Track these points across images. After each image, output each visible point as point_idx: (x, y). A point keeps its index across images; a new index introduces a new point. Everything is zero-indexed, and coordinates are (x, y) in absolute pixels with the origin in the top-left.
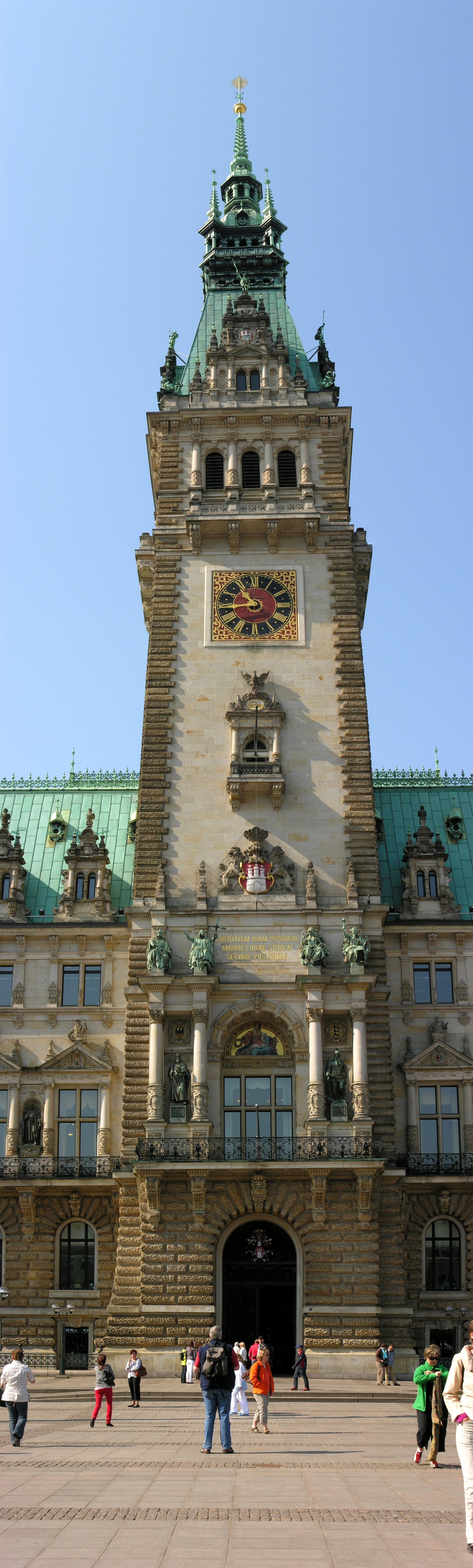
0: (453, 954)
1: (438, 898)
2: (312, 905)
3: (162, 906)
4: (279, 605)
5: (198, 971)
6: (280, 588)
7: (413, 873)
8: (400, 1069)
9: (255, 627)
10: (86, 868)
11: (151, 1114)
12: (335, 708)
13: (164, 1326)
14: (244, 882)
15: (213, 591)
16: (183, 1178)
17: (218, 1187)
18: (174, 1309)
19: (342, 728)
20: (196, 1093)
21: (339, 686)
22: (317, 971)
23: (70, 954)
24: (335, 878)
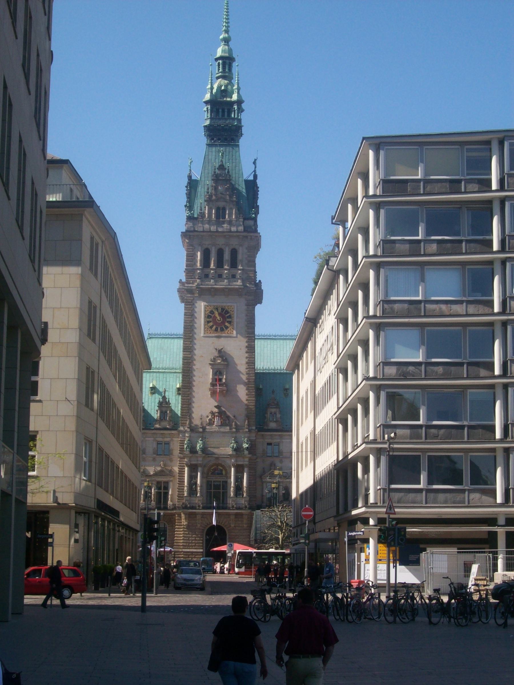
0: (279, 440)
1: (276, 422)
2: (234, 430)
3: (189, 430)
4: (228, 320)
5: (199, 451)
6: (228, 313)
7: (269, 413)
8: (261, 477)
9: (219, 329)
10: (164, 409)
11: (186, 494)
12: (244, 361)
13: (189, 555)
14: (214, 422)
15: (205, 313)
16: (195, 514)
17: (204, 516)
18: (191, 550)
19: (247, 369)
20: (199, 488)
21: (247, 352)
22: (234, 453)
23: (160, 439)
24: (242, 421)
